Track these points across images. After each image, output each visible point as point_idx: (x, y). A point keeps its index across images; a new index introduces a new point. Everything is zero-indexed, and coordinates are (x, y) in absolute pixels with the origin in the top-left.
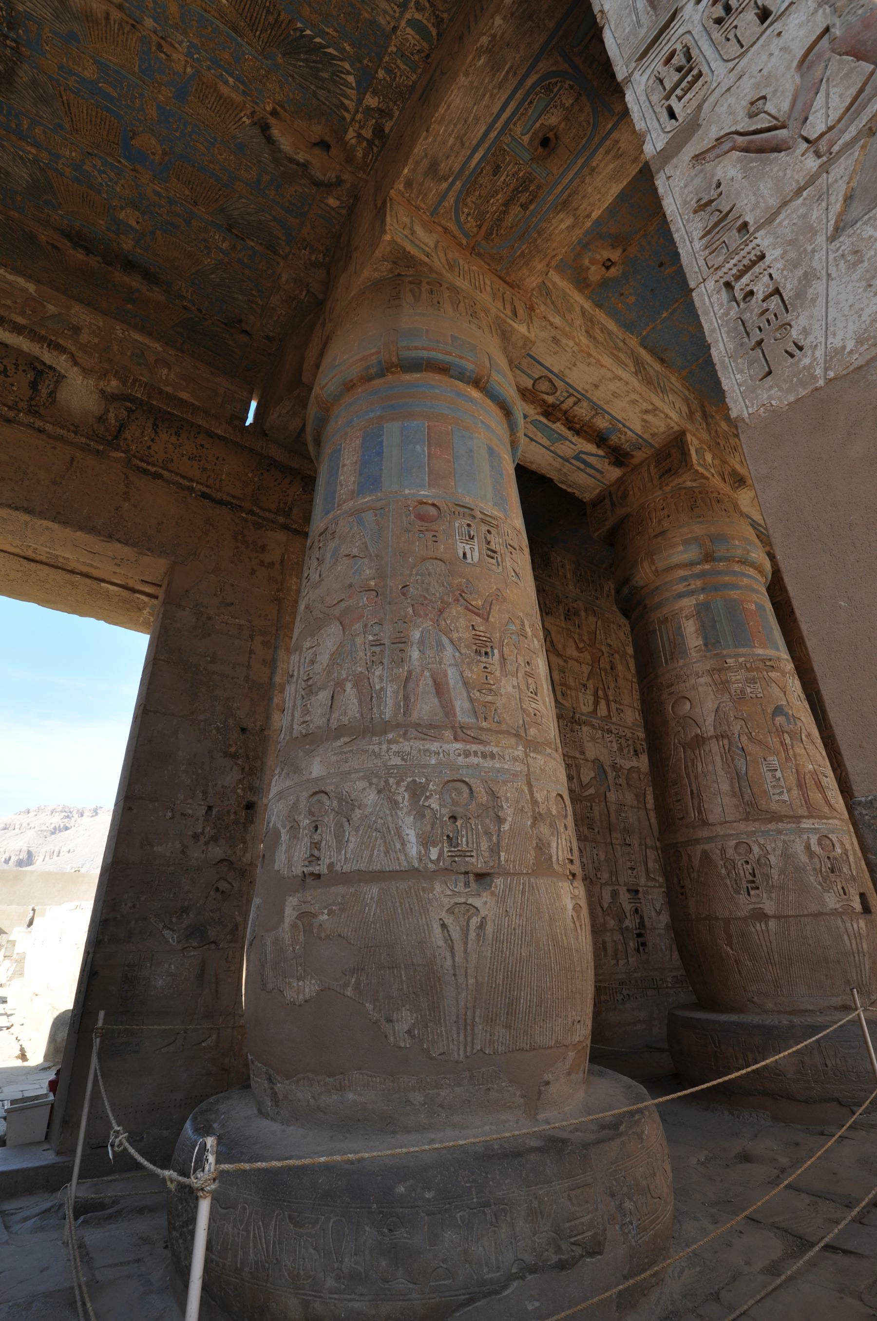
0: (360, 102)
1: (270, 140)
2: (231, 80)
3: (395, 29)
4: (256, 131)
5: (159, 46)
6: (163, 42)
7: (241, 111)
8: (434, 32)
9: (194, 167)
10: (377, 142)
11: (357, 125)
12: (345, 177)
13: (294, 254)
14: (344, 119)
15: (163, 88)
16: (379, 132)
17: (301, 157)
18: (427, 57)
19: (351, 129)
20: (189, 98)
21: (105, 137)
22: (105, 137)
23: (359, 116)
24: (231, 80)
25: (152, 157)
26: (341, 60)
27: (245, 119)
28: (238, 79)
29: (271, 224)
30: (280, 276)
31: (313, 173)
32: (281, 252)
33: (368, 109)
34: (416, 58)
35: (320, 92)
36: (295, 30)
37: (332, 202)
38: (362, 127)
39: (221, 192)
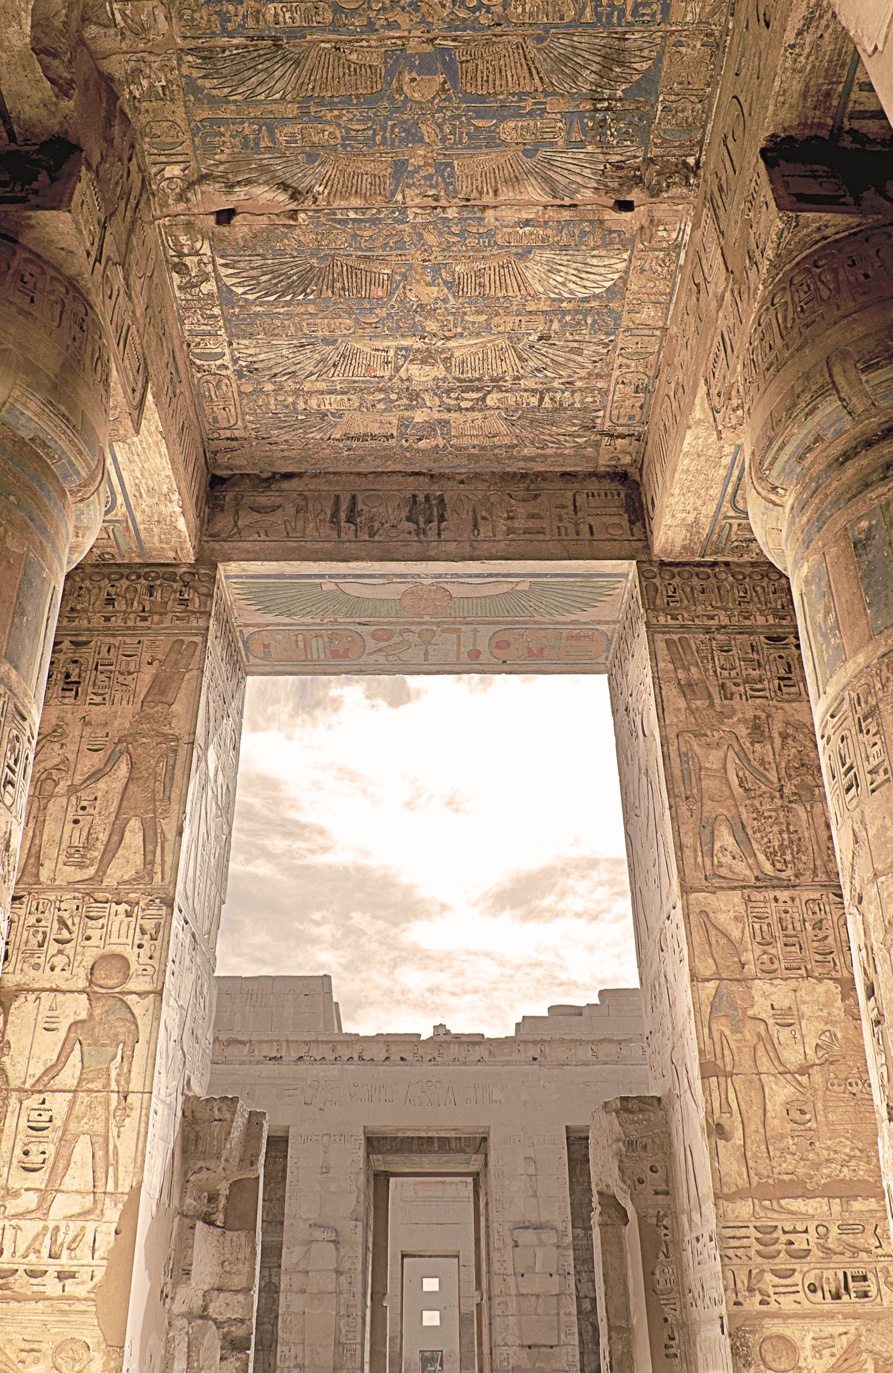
0: (218, 279)
1: (284, 186)
2: (352, 215)
3: (230, 344)
4: (302, 187)
5: (436, 198)
6: (434, 204)
7: (329, 194)
8: (198, 362)
9: (357, 97)
10: (176, 260)
11: (206, 261)
12: (182, 206)
13: (173, 69)
14: (222, 257)
15: (422, 163)
16: (181, 269)
17: (241, 192)
18: (189, 345)
19: (209, 254)
20: (389, 170)
21: (479, 62)
22: (479, 62)
23: (210, 268)
24: (352, 215)
25: (414, 75)
26: (258, 298)
27: (321, 189)
28: (344, 222)
29: (226, 90)
30: (168, 18)
31: (217, 186)
32: (190, 58)
33: (207, 280)
34: (197, 340)
35: (260, 263)
36: (313, 291)
37: (174, 171)
38: (200, 262)
39: (311, 86)
